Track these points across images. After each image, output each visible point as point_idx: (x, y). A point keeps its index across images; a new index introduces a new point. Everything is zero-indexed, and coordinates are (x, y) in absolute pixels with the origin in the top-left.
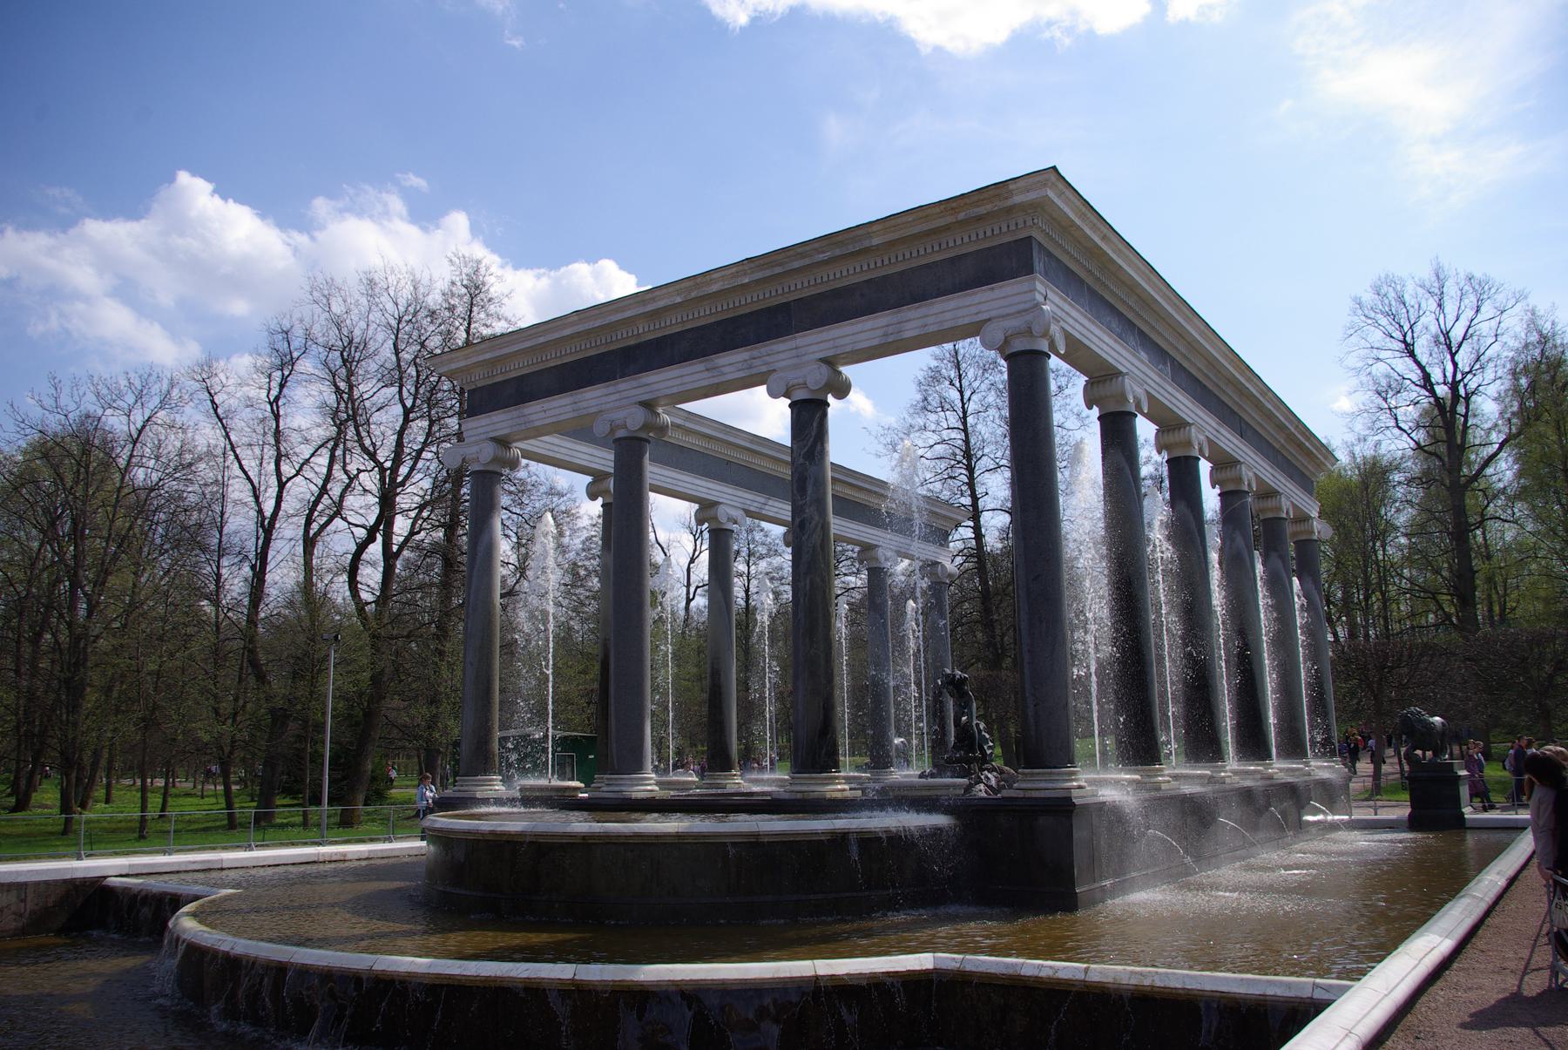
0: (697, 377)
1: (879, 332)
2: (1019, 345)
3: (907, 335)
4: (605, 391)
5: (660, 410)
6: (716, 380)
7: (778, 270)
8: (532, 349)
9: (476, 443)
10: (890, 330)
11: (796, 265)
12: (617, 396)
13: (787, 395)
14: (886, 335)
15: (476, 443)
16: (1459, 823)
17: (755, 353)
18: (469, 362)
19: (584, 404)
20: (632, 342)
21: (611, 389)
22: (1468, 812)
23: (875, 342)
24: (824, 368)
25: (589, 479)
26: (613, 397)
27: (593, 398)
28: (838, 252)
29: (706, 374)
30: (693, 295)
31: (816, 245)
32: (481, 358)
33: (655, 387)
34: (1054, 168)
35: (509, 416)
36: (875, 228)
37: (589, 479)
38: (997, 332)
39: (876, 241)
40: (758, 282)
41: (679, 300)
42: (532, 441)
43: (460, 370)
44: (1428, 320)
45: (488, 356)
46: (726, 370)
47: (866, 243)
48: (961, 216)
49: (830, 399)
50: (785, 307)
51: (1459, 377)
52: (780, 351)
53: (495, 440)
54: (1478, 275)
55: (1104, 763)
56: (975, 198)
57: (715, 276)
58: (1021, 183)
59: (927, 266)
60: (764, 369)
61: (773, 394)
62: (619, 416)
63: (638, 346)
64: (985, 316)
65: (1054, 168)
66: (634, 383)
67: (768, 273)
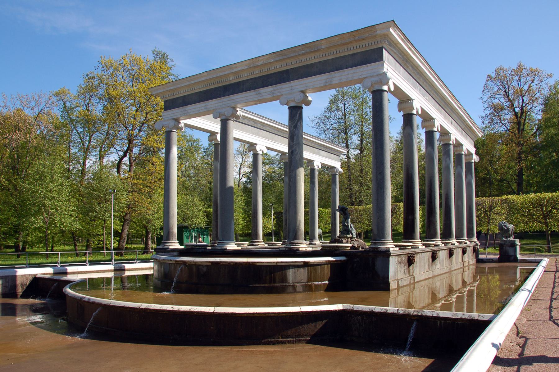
2: (376, 88)
3: (334, 83)
5: (238, 109)
6: (260, 98)
7: (286, 57)
8: (189, 85)
9: (168, 120)
11: (292, 55)
12: (222, 104)
13: (287, 104)
15: (168, 120)
16: (515, 260)
17: (275, 88)
18: (165, 90)
19: (209, 107)
20: (227, 83)
21: (220, 101)
22: (519, 257)
23: (322, 85)
24: (302, 94)
25: (209, 134)
26: (220, 104)
27: (212, 103)
29: (256, 96)
30: (252, 66)
31: (300, 48)
32: (169, 89)
34: (393, 21)
36: (323, 42)
37: (209, 134)
38: (368, 83)
40: (277, 61)
41: (246, 68)
42: (188, 120)
43: (162, 93)
44: (515, 83)
45: (172, 88)
46: (263, 94)
49: (303, 106)
50: (287, 71)
51: (524, 105)
52: (285, 88)
53: (174, 119)
54: (534, 68)
57: (260, 59)
58: (380, 26)
59: (343, 57)
60: (279, 94)
61: (282, 104)
64: (364, 76)
65: (393, 21)
67: (281, 58)
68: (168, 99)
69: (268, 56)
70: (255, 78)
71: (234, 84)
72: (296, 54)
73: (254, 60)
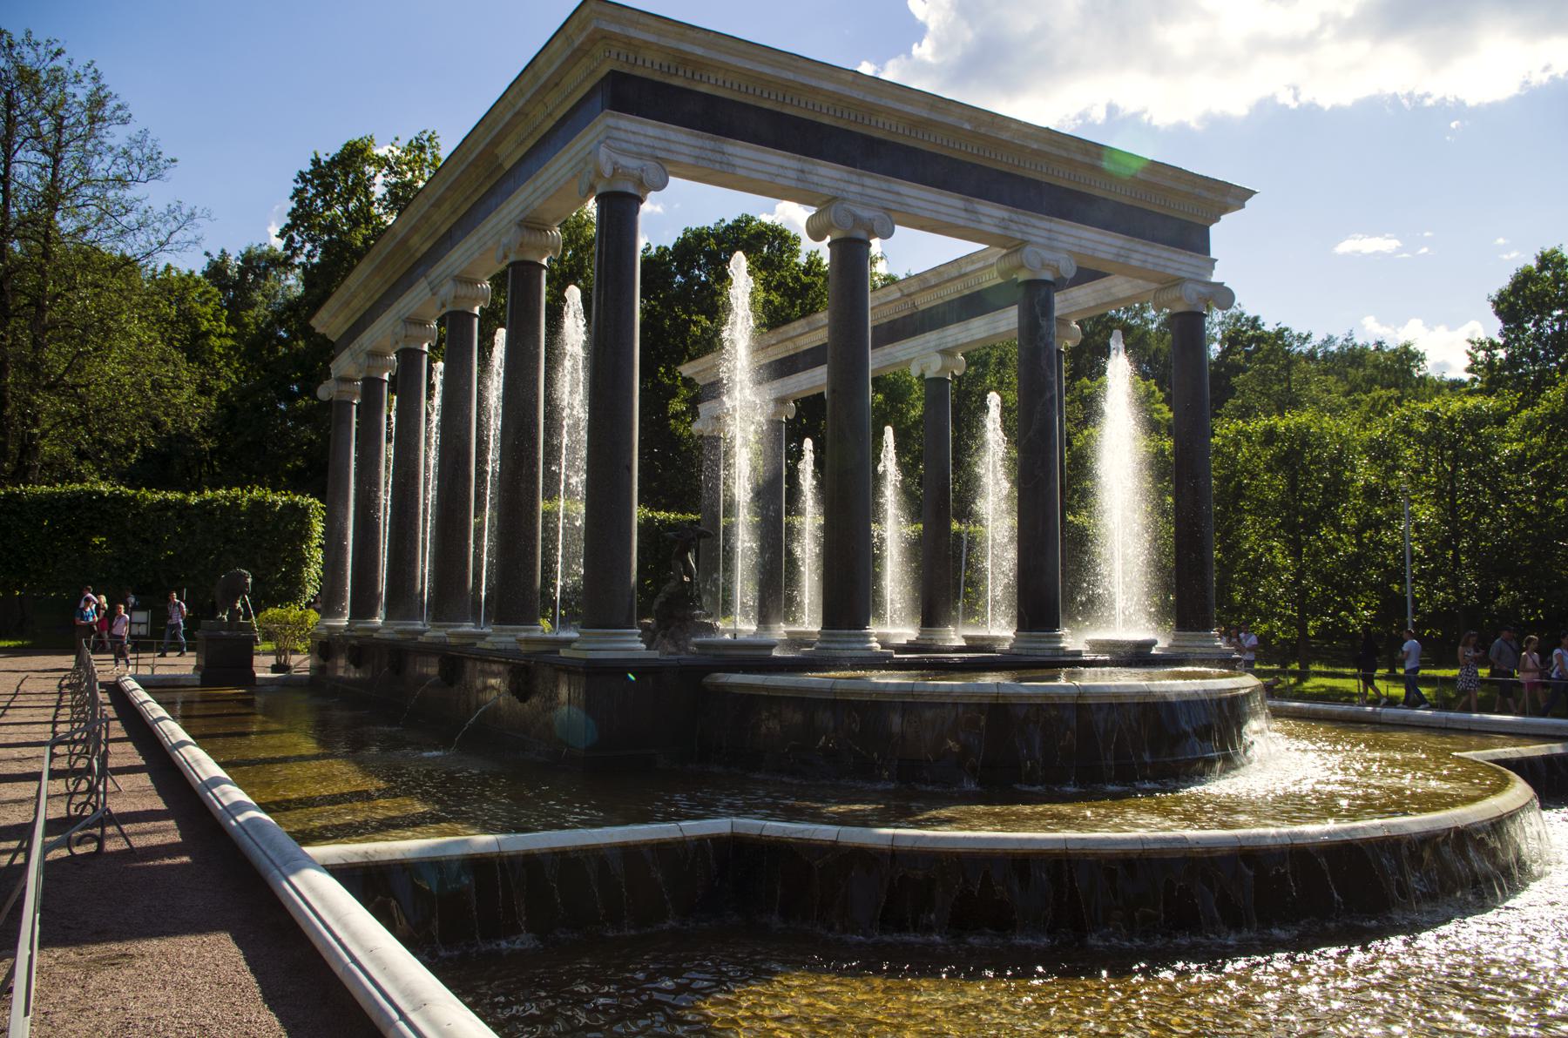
0: (951, 211)
1: (1114, 250)
3: (1133, 262)
4: (845, 176)
7: (1064, 154)
11: (1079, 157)
14: (1118, 255)
15: (640, 156)
17: (1014, 216)
19: (816, 179)
20: (878, 134)
21: (854, 178)
26: (853, 188)
27: (827, 174)
29: (963, 214)
30: (983, 130)
33: (910, 201)
35: (693, 141)
41: (967, 126)
55: (893, 622)
66: (884, 185)
68: (638, 72)
71: (897, 147)
72: (1087, 160)
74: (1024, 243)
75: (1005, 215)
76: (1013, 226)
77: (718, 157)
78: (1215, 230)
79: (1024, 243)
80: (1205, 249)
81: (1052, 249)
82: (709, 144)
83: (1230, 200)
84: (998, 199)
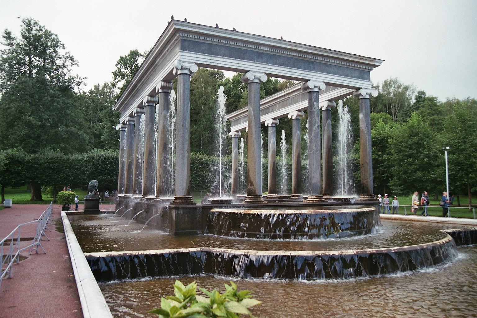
4: (252, 64)
7: (320, 53)
10: (341, 81)
21: (254, 64)
28: (336, 56)
29: (289, 73)
30: (294, 48)
36: (347, 55)
39: (345, 58)
41: (289, 47)
47: (343, 57)
48: (364, 62)
50: (313, 62)
56: (369, 59)
58: (378, 61)
62: (258, 75)
63: (262, 53)
68: (189, 39)
69: (309, 47)
70: (287, 57)
71: (268, 54)
73: (298, 45)
74: (309, 80)
75: (303, 72)
76: (305, 75)
77: (213, 61)
78: (371, 72)
79: (309, 80)
80: (369, 79)
81: (317, 81)
82: (210, 58)
83: (375, 64)
84: (300, 68)
